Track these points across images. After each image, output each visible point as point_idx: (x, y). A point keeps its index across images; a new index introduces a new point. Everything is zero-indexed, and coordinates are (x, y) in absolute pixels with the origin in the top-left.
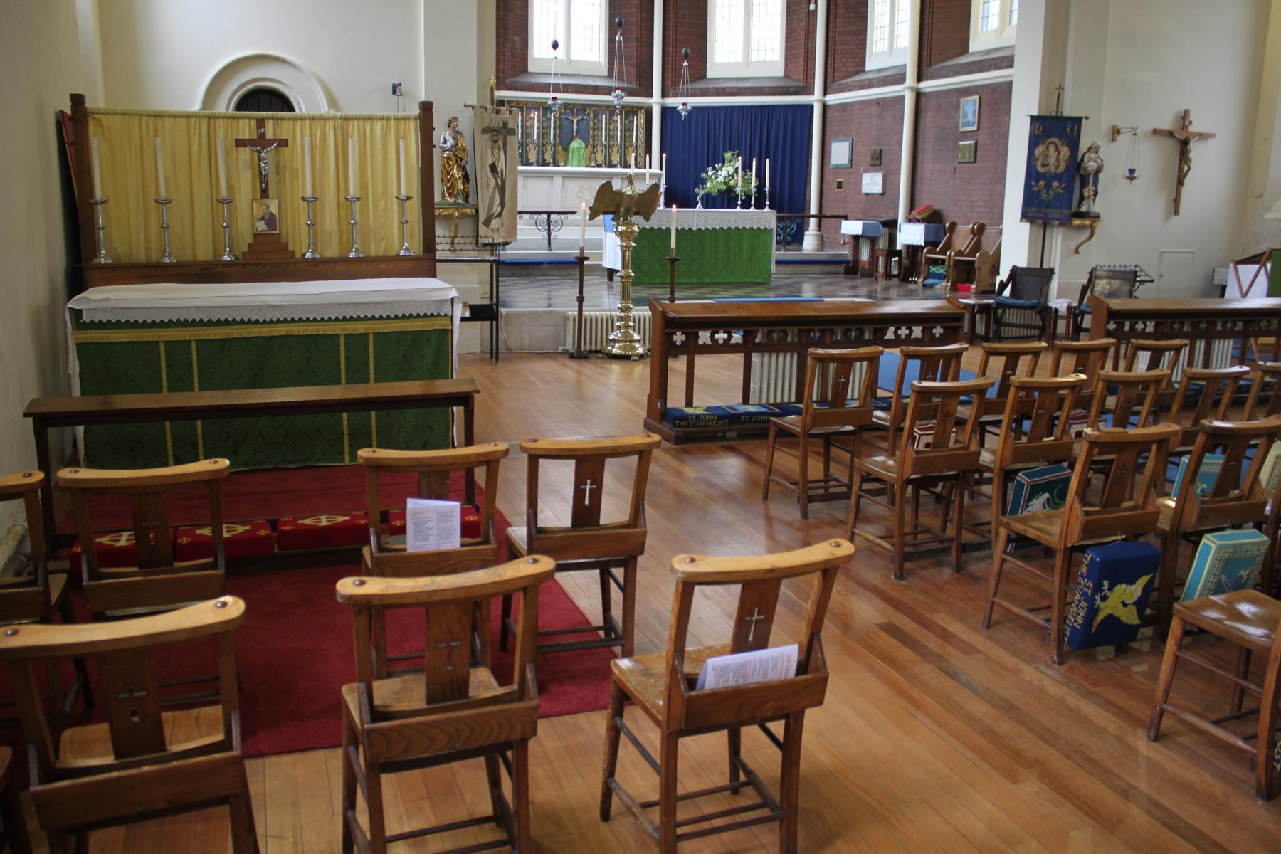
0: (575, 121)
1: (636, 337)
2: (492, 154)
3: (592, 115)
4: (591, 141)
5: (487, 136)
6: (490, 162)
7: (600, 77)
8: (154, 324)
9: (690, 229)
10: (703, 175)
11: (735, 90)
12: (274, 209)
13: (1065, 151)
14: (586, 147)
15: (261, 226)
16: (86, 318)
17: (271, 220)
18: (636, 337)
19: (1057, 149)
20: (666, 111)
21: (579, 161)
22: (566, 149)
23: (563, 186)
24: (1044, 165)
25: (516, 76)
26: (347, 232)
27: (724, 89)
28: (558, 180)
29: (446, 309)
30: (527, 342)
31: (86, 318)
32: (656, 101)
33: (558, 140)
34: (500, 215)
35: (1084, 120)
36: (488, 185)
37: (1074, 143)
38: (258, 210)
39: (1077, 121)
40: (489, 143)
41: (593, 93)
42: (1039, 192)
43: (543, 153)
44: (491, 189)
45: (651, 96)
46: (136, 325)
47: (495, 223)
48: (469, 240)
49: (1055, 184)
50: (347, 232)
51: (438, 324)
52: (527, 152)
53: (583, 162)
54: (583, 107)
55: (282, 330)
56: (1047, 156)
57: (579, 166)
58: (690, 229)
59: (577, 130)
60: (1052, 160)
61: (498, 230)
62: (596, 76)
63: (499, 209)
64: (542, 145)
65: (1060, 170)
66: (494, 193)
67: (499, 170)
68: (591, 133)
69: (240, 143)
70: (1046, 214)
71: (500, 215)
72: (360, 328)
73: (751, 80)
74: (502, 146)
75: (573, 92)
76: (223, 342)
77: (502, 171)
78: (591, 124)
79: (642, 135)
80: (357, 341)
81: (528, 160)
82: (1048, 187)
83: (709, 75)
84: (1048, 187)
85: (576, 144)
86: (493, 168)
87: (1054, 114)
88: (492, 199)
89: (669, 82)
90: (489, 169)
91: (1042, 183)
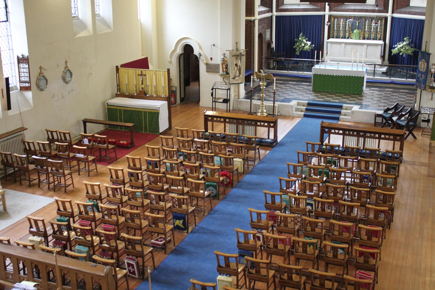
0: (357, 22)
1: (265, 111)
2: (236, 61)
3: (364, 20)
4: (363, 30)
5: (234, 57)
6: (235, 63)
7: (371, 5)
8: (117, 106)
9: (333, 75)
10: (394, 46)
11: (414, 13)
12: (143, 87)
13: (426, 64)
14: (361, 32)
15: (141, 89)
16: (108, 104)
17: (143, 88)
18: (265, 111)
19: (424, 64)
20: (393, 18)
21: (355, 37)
22: (353, 32)
23: (345, 47)
24: (421, 68)
25: (338, 6)
26: (156, 92)
27: (411, 12)
28: (343, 45)
29: (158, 109)
30: (244, 108)
31: (108, 104)
32: (389, 15)
33: (351, 29)
34: (239, 76)
35: (431, 55)
36: (234, 69)
37: (428, 62)
38: (141, 87)
39: (430, 54)
40: (235, 59)
41: (366, 12)
42: (419, 77)
43: (345, 34)
44: (236, 70)
45: (387, 12)
46: (114, 106)
47: (237, 78)
48: (223, 83)
49: (423, 75)
50: (156, 92)
51: (157, 111)
52: (339, 33)
53: (358, 38)
54: (360, 18)
55: (134, 109)
56: (421, 65)
57: (356, 39)
58: (333, 75)
59: (358, 26)
60: (423, 67)
61: (238, 80)
62: (370, 5)
63: (239, 75)
64: (345, 31)
65: (424, 71)
66: (236, 71)
67: (238, 65)
68: (363, 27)
69: (138, 75)
70: (420, 85)
71: (239, 76)
72: (145, 110)
73: (422, 8)
74: (239, 59)
75: (358, 12)
76: (126, 110)
77: (239, 65)
78: (364, 24)
79: (383, 27)
80: (145, 112)
81: (339, 36)
82: (421, 76)
83: (411, 4)
84: (421, 76)
85: (355, 31)
86: (236, 65)
87: (424, 51)
88: (236, 72)
89: (395, 7)
90: (235, 65)
91: (420, 74)
